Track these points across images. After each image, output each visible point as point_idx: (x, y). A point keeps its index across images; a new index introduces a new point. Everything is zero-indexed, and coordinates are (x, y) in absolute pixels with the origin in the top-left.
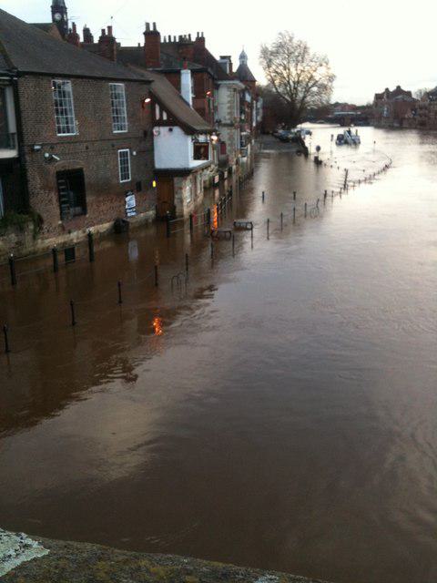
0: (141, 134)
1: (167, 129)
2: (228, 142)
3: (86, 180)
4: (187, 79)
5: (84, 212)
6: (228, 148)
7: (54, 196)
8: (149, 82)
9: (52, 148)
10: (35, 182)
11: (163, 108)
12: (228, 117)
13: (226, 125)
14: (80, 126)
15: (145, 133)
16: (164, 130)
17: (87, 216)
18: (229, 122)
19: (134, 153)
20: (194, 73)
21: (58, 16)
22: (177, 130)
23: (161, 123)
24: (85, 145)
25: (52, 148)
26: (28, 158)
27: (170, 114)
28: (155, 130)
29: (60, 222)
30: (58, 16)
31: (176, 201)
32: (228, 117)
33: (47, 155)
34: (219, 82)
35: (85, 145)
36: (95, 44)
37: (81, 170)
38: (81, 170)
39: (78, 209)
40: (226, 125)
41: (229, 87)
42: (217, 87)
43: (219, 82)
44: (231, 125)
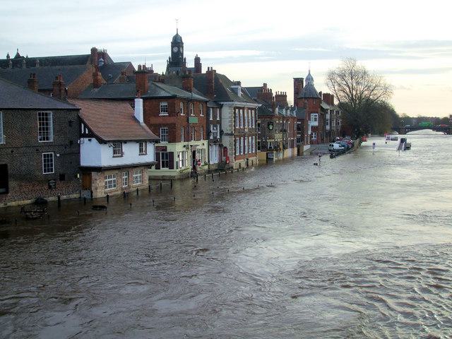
0: (67, 142)
1: (87, 139)
2: (229, 148)
4: (139, 103)
5: (7, 192)
6: (229, 152)
8: (78, 110)
14: (6, 139)
15: (71, 143)
17: (9, 194)
18: (230, 132)
19: (58, 155)
20: (145, 100)
22: (94, 140)
23: (85, 136)
24: (10, 150)
28: (82, 139)
30: (176, 50)
34: (222, 103)
35: (10, 150)
36: (190, 70)
37: (5, 166)
38: (5, 166)
41: (230, 107)
42: (221, 107)
43: (222, 103)
44: (231, 134)
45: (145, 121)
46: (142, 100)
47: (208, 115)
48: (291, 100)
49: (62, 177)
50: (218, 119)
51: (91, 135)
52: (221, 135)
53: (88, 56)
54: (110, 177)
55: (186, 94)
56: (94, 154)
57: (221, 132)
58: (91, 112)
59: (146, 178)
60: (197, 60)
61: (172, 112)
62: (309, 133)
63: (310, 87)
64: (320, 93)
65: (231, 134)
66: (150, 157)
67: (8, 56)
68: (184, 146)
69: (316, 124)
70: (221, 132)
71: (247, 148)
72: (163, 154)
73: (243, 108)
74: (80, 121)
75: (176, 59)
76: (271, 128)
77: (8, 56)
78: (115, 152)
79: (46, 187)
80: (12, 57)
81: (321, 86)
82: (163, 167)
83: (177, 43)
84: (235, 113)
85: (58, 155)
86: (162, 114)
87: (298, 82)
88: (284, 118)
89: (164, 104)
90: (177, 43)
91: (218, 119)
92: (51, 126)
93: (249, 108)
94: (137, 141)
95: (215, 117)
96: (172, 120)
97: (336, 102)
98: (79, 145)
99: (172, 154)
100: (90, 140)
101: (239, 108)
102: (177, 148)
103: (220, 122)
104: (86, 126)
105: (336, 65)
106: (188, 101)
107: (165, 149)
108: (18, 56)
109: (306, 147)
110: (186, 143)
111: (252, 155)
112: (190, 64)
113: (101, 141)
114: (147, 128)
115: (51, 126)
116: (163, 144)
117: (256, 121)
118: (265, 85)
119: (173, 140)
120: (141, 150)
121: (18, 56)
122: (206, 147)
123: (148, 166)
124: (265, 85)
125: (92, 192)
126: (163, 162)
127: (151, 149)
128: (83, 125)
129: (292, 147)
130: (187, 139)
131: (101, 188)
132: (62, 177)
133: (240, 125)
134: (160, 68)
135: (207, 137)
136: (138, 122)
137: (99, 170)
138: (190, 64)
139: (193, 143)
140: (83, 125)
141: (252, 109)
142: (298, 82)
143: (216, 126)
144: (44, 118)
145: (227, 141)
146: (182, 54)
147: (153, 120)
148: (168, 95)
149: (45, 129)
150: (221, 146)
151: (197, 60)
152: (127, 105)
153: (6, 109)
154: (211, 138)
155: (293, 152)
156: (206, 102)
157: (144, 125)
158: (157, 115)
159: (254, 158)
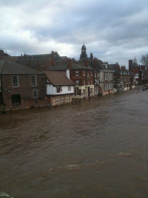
3: (21, 97)
4: (68, 72)
5: (20, 104)
6: (102, 89)
7: (10, 100)
8: (45, 74)
9: (11, 90)
10: (5, 97)
11: (48, 80)
12: (102, 80)
13: (102, 82)
15: (43, 86)
16: (49, 85)
17: (21, 105)
18: (102, 82)
20: (70, 70)
22: (51, 85)
23: (48, 84)
25: (11, 90)
26: (3, 92)
27: (50, 82)
28: (47, 85)
29: (12, 106)
30: (83, 51)
31: (51, 103)
32: (102, 80)
33: (9, 91)
35: (21, 89)
39: (19, 103)
40: (102, 82)
41: (102, 72)
42: (99, 72)
44: (103, 83)
45: (70, 78)
46: (69, 70)
47: (94, 76)
48: (127, 68)
49: (40, 99)
50: (98, 77)
51: (50, 83)
52: (99, 83)
54: (57, 99)
55: (86, 68)
56: (51, 90)
57: (99, 82)
58: (51, 75)
59: (71, 99)
60: (91, 55)
61: (80, 74)
62: (135, 81)
63: (135, 64)
64: (140, 65)
65: (103, 83)
66: (72, 91)
67: (22, 55)
68: (85, 87)
69: (137, 77)
70: (99, 82)
71: (109, 87)
72: (77, 90)
73: (108, 73)
74: (46, 78)
75: (84, 55)
76: (119, 80)
77: (22, 55)
79: (35, 102)
80: (23, 55)
81: (140, 63)
82: (77, 95)
83: (84, 48)
84: (104, 74)
85: (39, 91)
86: (76, 76)
87: (130, 62)
88: (124, 76)
89: (77, 72)
90: (84, 48)
91: (98, 77)
92: (18, 81)
93: (110, 72)
94: (67, 86)
95: (97, 76)
96: (80, 78)
97: (146, 68)
98: (46, 87)
99: (80, 90)
100: (50, 85)
101: (106, 72)
102: (83, 88)
103: (99, 78)
104: (48, 80)
106: (86, 70)
107: (78, 88)
108: (25, 55)
109: (133, 87)
110: (86, 86)
111: (111, 90)
112: (89, 56)
113: (54, 86)
114: (71, 80)
115: (18, 81)
116: (77, 86)
117: (113, 77)
118: (117, 63)
119: (81, 84)
120: (69, 88)
121: (25, 55)
122: (93, 87)
123: (71, 94)
124: (117, 63)
125: (51, 104)
126: (77, 93)
127: (72, 88)
128: (47, 80)
129: (128, 87)
130: (86, 84)
131: (54, 102)
132: (40, 99)
133: (106, 79)
136: (68, 78)
137: (54, 96)
138: (89, 56)
139: (88, 86)
140: (47, 80)
141: (111, 73)
142: (130, 62)
143: (97, 79)
144: (33, 77)
145: (101, 85)
146: (86, 52)
147: (74, 78)
148: (79, 68)
149: (34, 81)
150: (99, 87)
151: (91, 55)
152: (64, 72)
153: (20, 74)
154: (96, 84)
155: (128, 88)
156: (93, 70)
157: (70, 79)
158: (75, 75)
159: (112, 91)
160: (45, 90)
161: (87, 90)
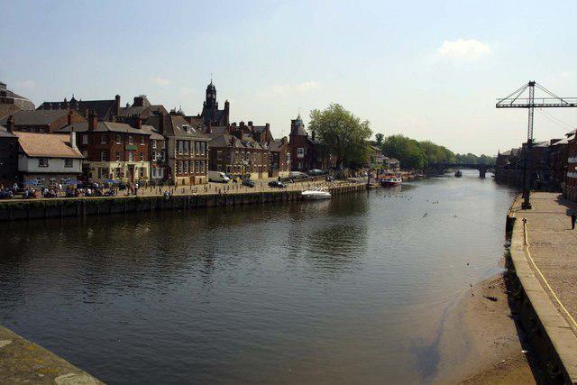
21: (209, 96)
53: (113, 101)
57: (167, 156)
60: (227, 104)
67: (65, 100)
69: (301, 156)
70: (167, 156)
75: (210, 102)
77: (65, 100)
78: (40, 164)
80: (69, 100)
83: (211, 91)
90: (211, 91)
93: (196, 142)
105: (323, 107)
108: (73, 99)
112: (221, 107)
118: (268, 125)
121: (73, 99)
124: (268, 125)
134: (195, 108)
135: (150, 159)
138: (221, 107)
142: (296, 125)
146: (215, 100)
151: (227, 104)
160: (17, 164)
161: (126, 170)
